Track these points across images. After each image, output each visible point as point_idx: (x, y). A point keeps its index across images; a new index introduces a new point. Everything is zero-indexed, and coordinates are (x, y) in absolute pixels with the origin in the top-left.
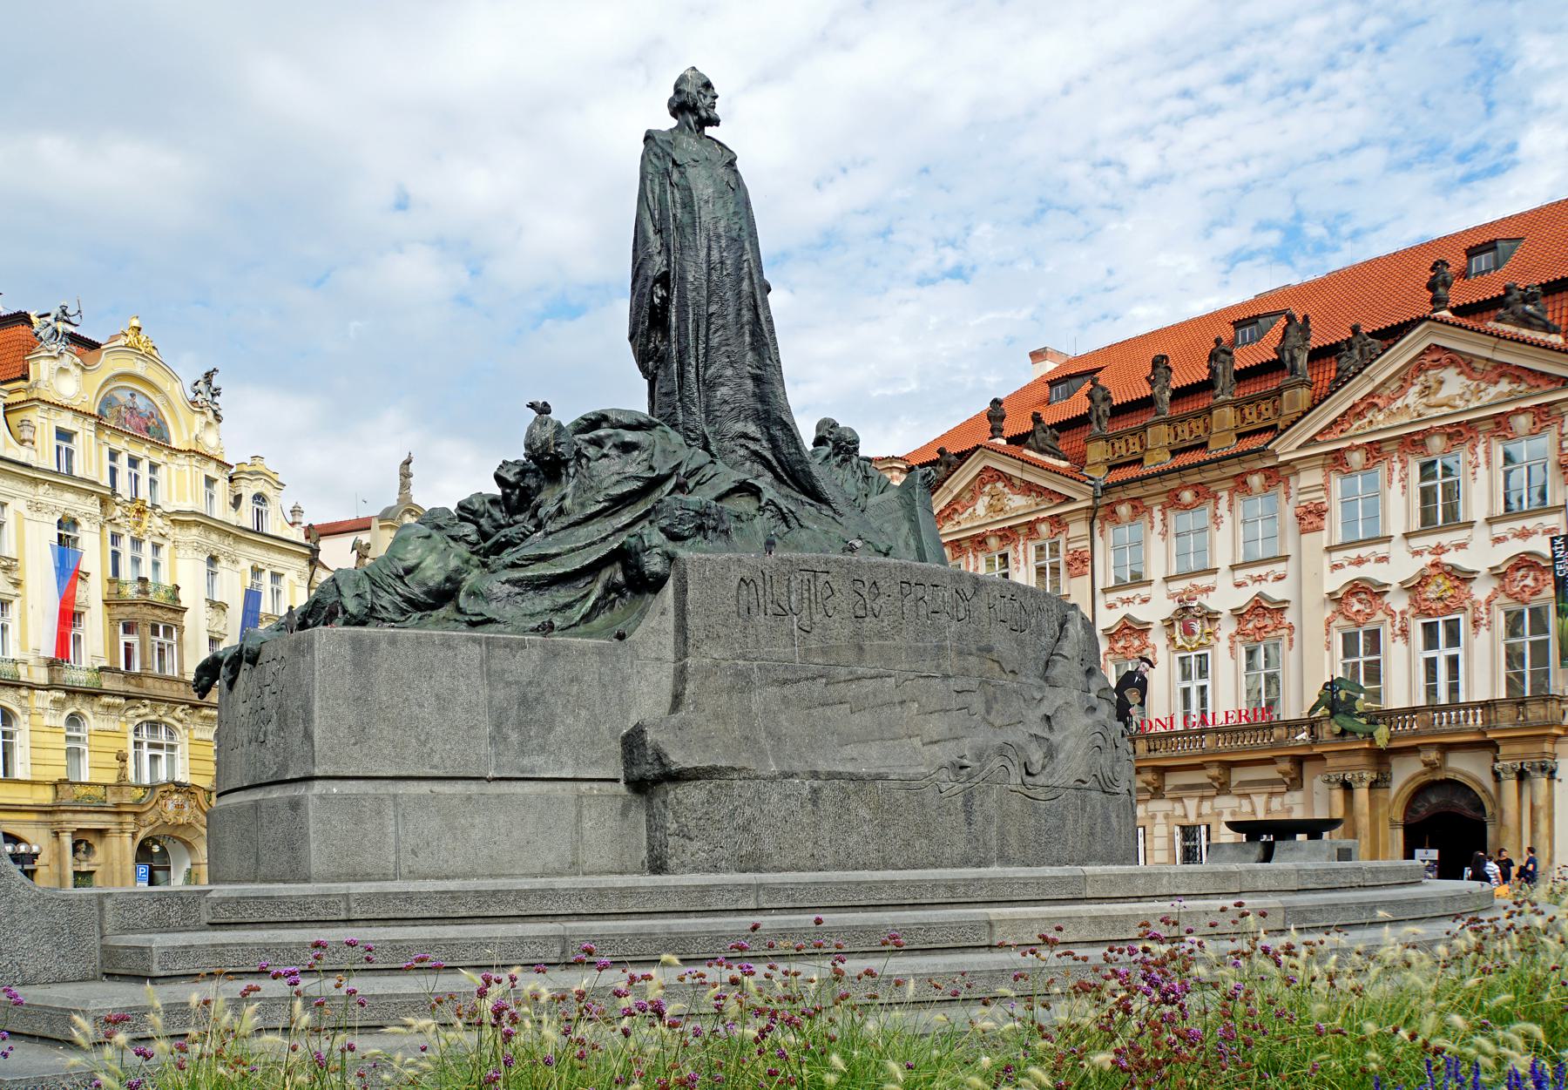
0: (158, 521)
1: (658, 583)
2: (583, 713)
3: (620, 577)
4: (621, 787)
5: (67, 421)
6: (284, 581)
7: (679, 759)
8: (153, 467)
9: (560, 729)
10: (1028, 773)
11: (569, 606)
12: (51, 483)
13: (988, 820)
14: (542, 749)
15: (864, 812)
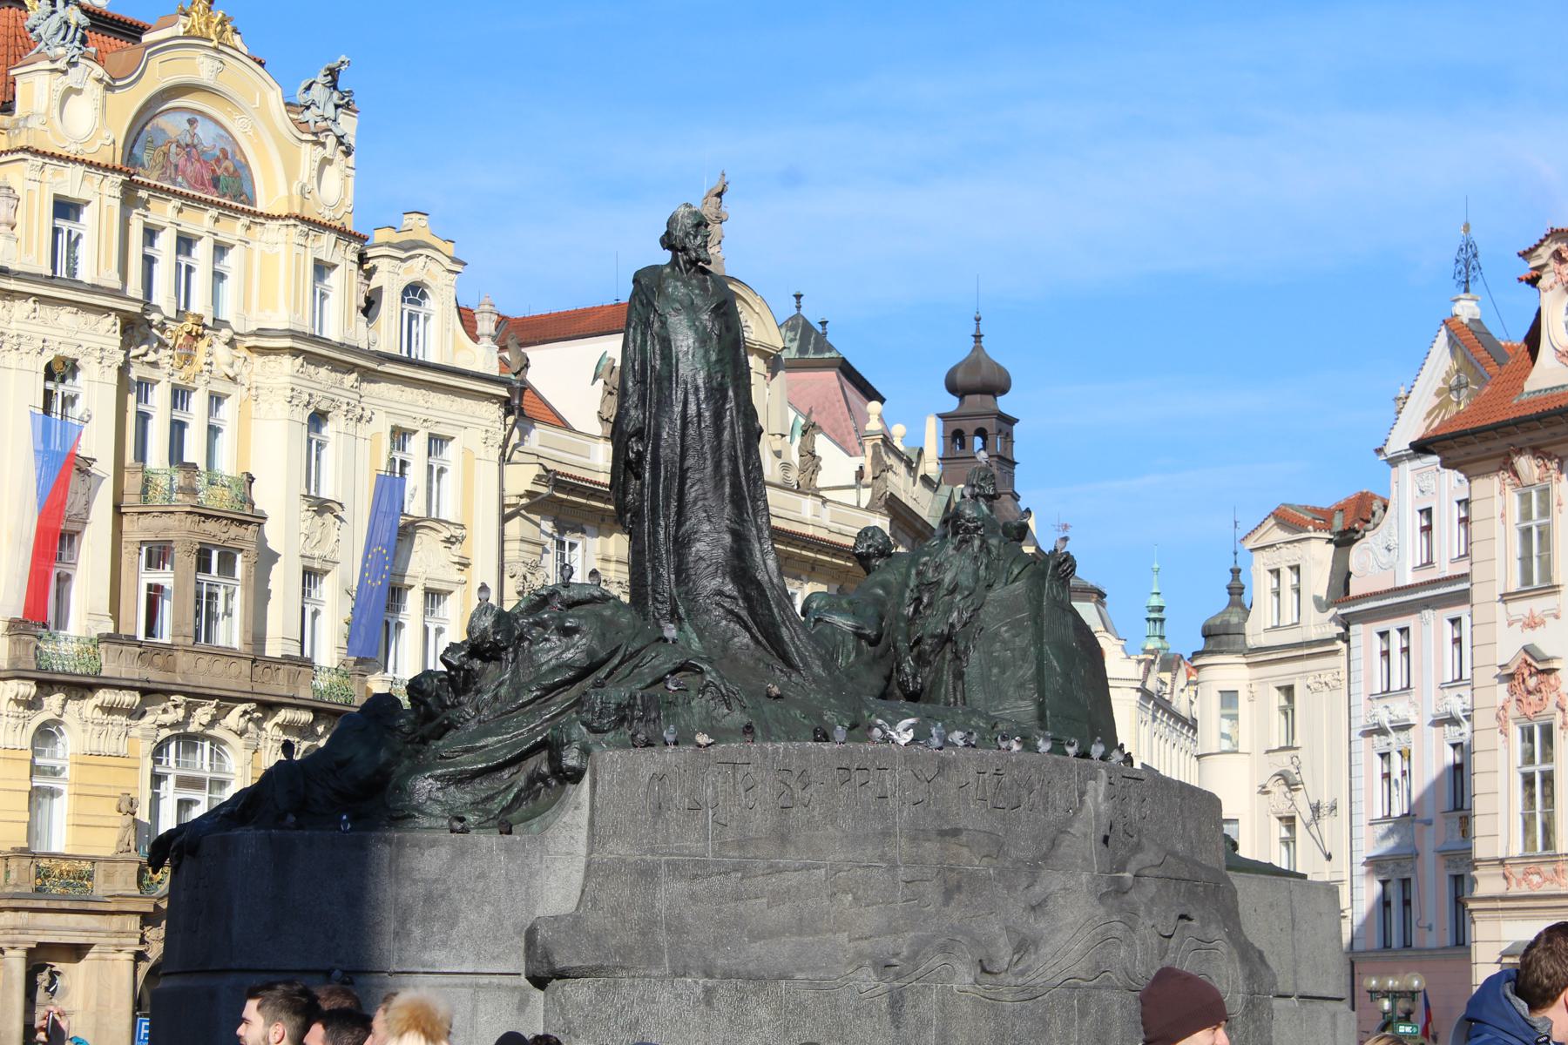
0: (222, 353)
1: (576, 776)
2: (487, 908)
3: (545, 769)
4: (523, 981)
5: (71, 182)
6: (451, 452)
7: (561, 961)
8: (220, 249)
9: (463, 925)
10: (984, 970)
11: (490, 798)
12: (42, 299)
13: (923, 1024)
14: (444, 944)
15: (763, 1013)
